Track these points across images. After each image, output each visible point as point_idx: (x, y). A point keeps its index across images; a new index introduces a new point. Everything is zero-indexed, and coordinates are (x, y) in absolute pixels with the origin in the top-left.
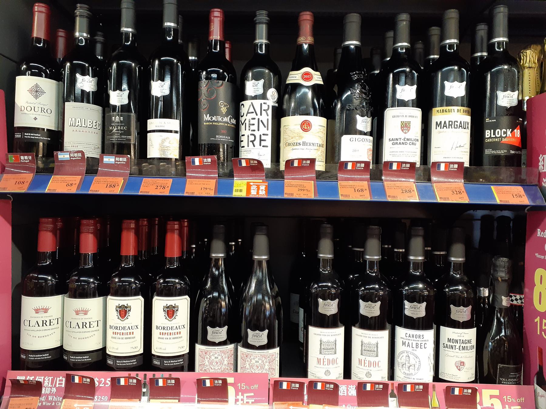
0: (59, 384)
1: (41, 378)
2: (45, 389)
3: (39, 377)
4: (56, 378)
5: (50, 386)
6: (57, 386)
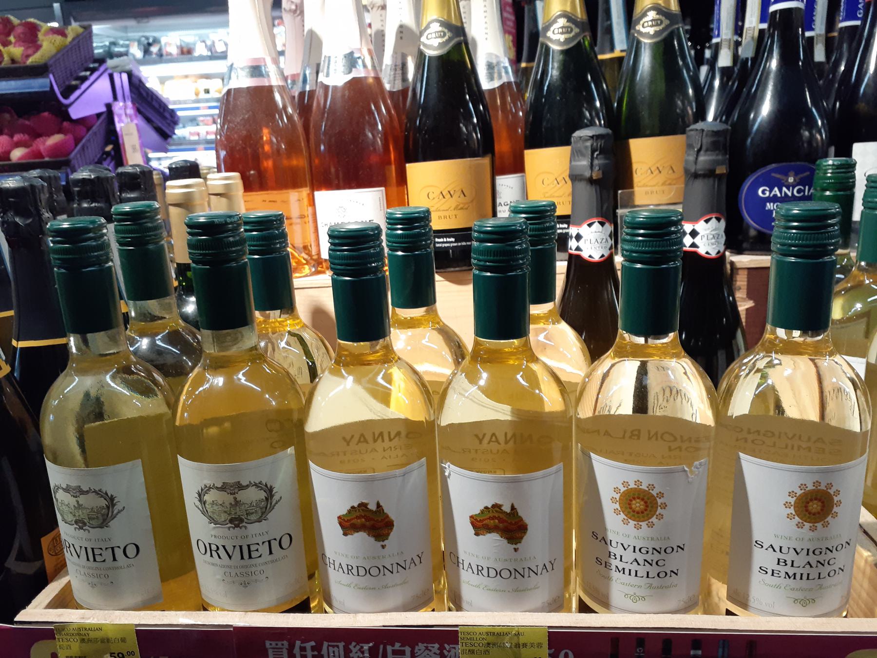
1: (338, 647)
3: (330, 644)
4: (381, 647)
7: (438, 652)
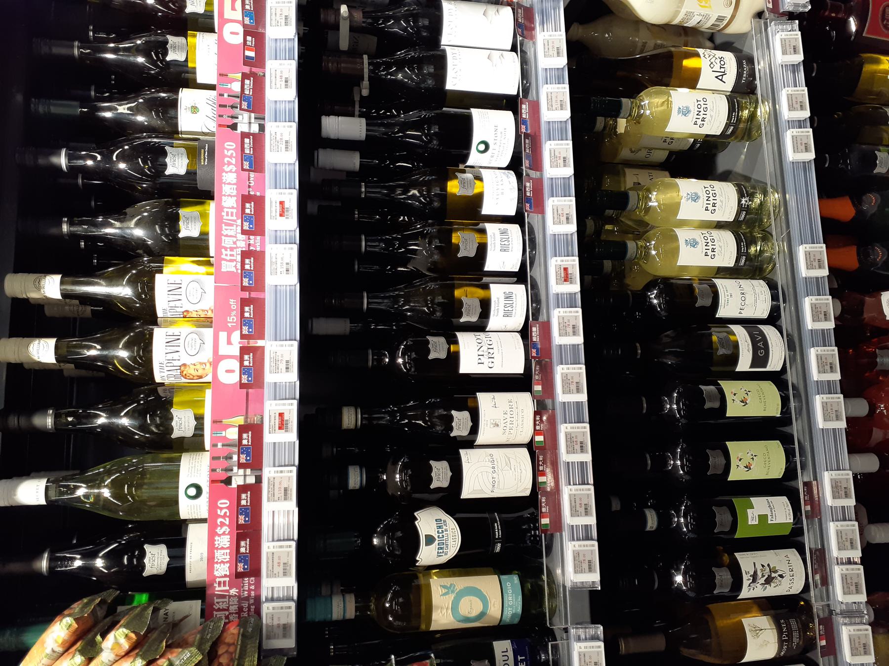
0: (225, 585)
2: (232, 605)
5: (227, 600)
6: (227, 588)
7: (219, 565)
